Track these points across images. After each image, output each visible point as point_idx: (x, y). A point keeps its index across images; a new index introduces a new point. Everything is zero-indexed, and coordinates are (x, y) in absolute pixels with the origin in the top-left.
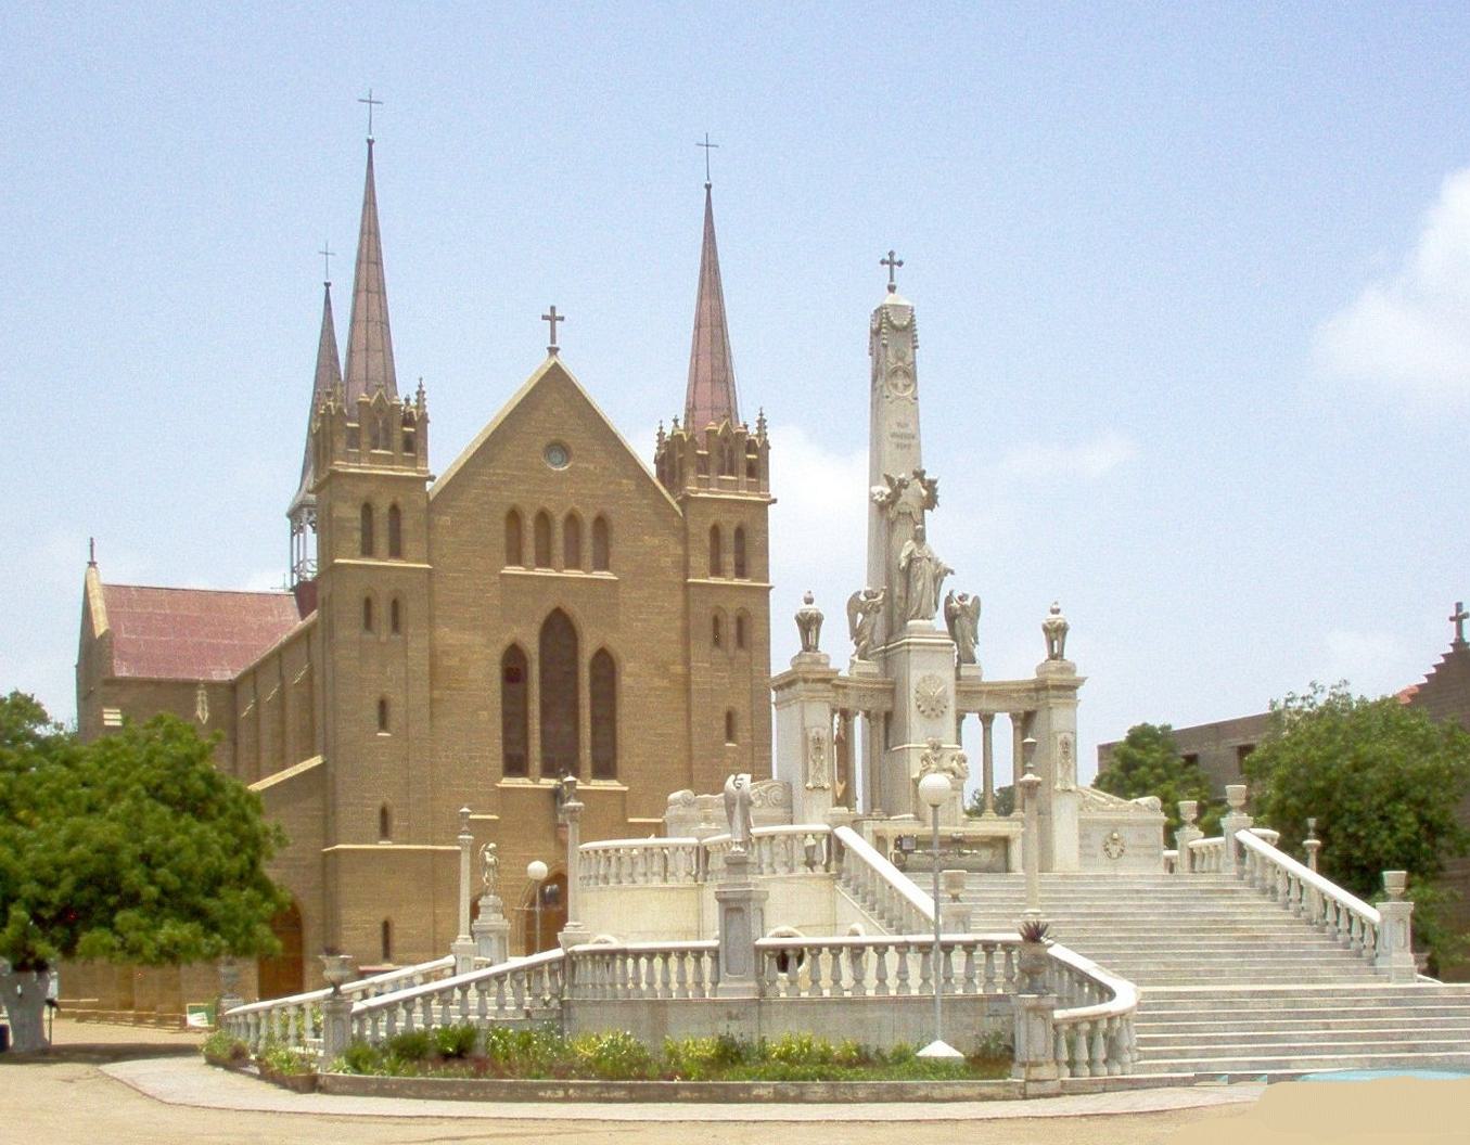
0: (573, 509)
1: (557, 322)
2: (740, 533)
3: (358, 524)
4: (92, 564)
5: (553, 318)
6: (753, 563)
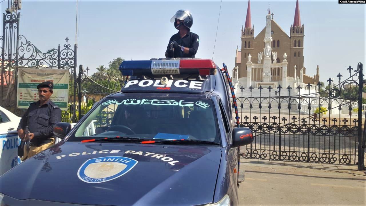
2: (299, 41)
3: (244, 44)
4: (237, 49)
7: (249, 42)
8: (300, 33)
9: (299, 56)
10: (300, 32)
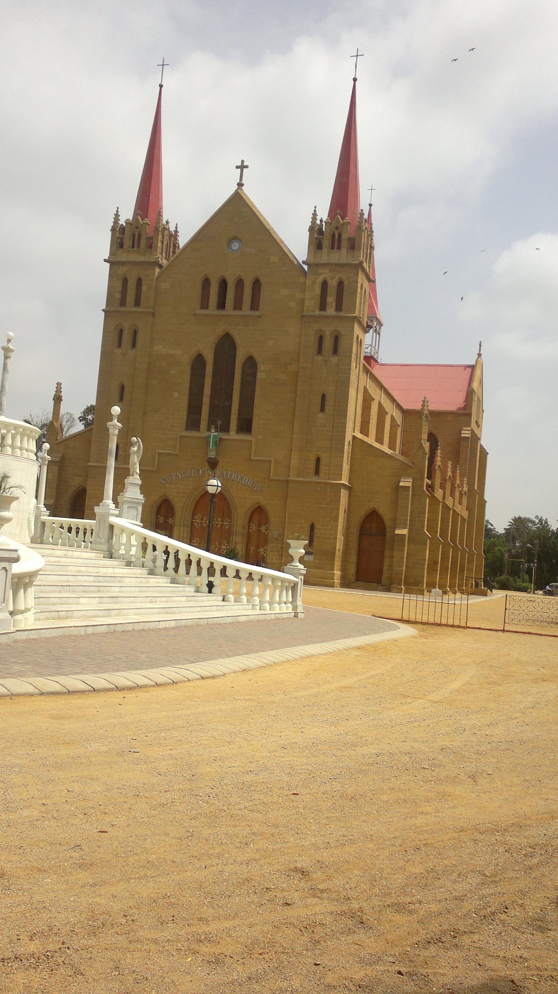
0: (240, 275)
1: (244, 169)
5: (242, 167)
6: (345, 303)
7: (139, 282)
8: (344, 250)
9: (335, 351)
10: (344, 244)
